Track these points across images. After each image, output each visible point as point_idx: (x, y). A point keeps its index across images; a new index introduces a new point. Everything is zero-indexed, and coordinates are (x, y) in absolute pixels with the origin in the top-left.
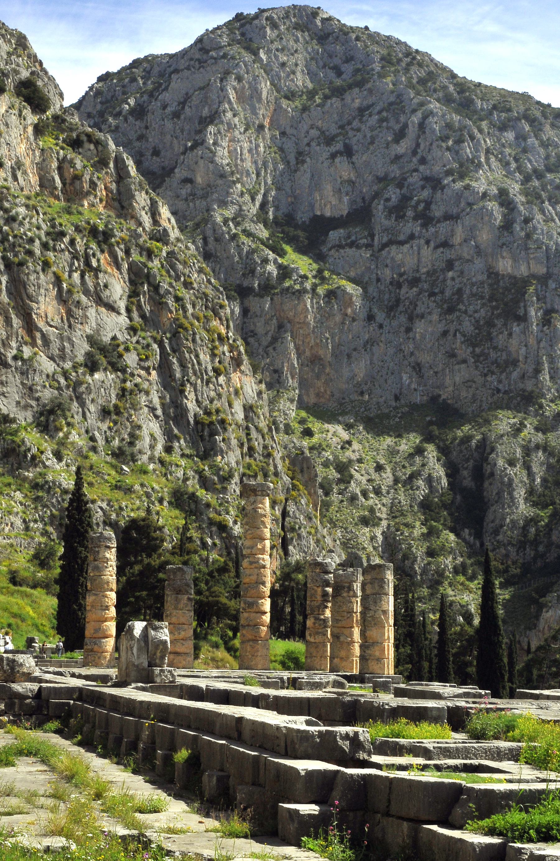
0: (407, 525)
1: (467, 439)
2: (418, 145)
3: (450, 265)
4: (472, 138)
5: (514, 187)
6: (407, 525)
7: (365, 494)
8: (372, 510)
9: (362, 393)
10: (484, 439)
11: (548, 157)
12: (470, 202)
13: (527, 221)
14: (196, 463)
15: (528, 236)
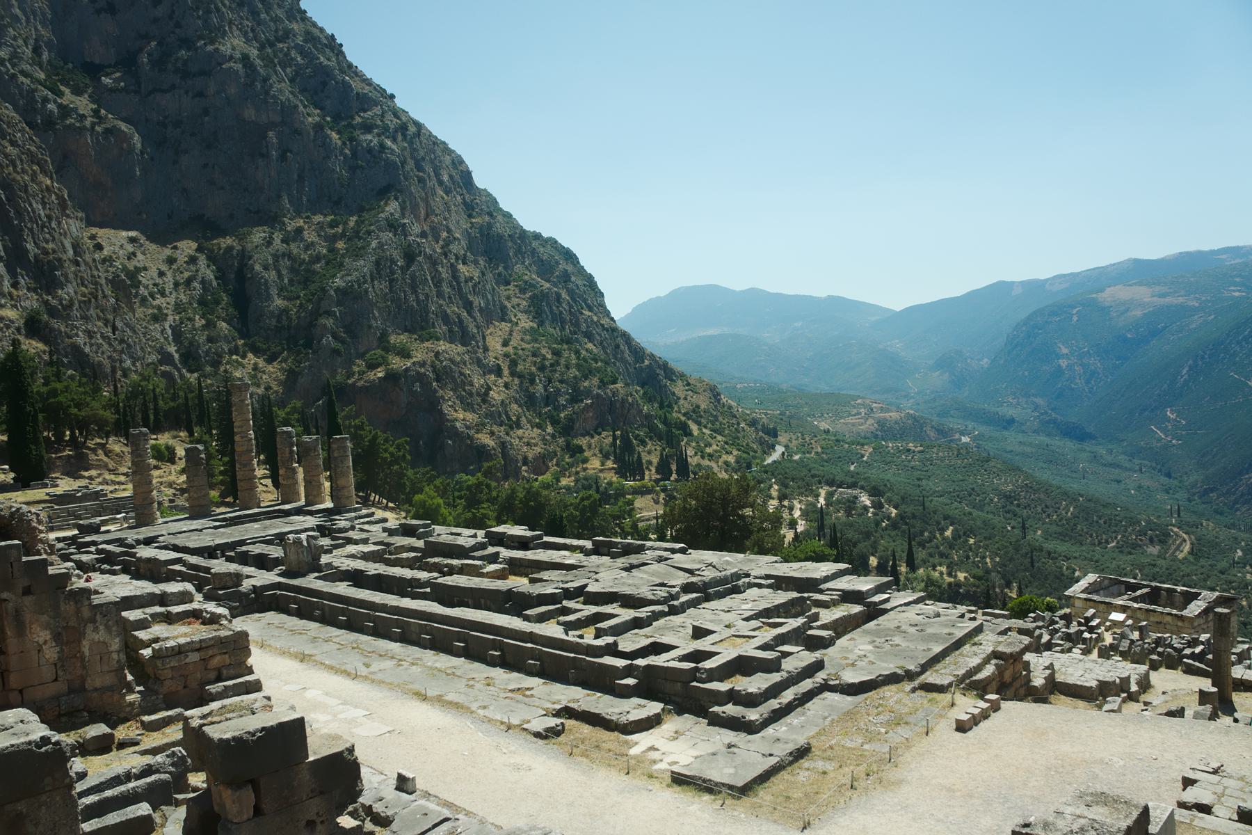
0: (189, 319)
1: (230, 248)
2: (173, 12)
3: (206, 112)
4: (218, 10)
5: (254, 53)
6: (189, 319)
7: (152, 296)
8: (159, 308)
9: (140, 214)
10: (243, 250)
11: (276, 31)
12: (217, 59)
13: (265, 80)
14: (41, 295)
15: (267, 93)
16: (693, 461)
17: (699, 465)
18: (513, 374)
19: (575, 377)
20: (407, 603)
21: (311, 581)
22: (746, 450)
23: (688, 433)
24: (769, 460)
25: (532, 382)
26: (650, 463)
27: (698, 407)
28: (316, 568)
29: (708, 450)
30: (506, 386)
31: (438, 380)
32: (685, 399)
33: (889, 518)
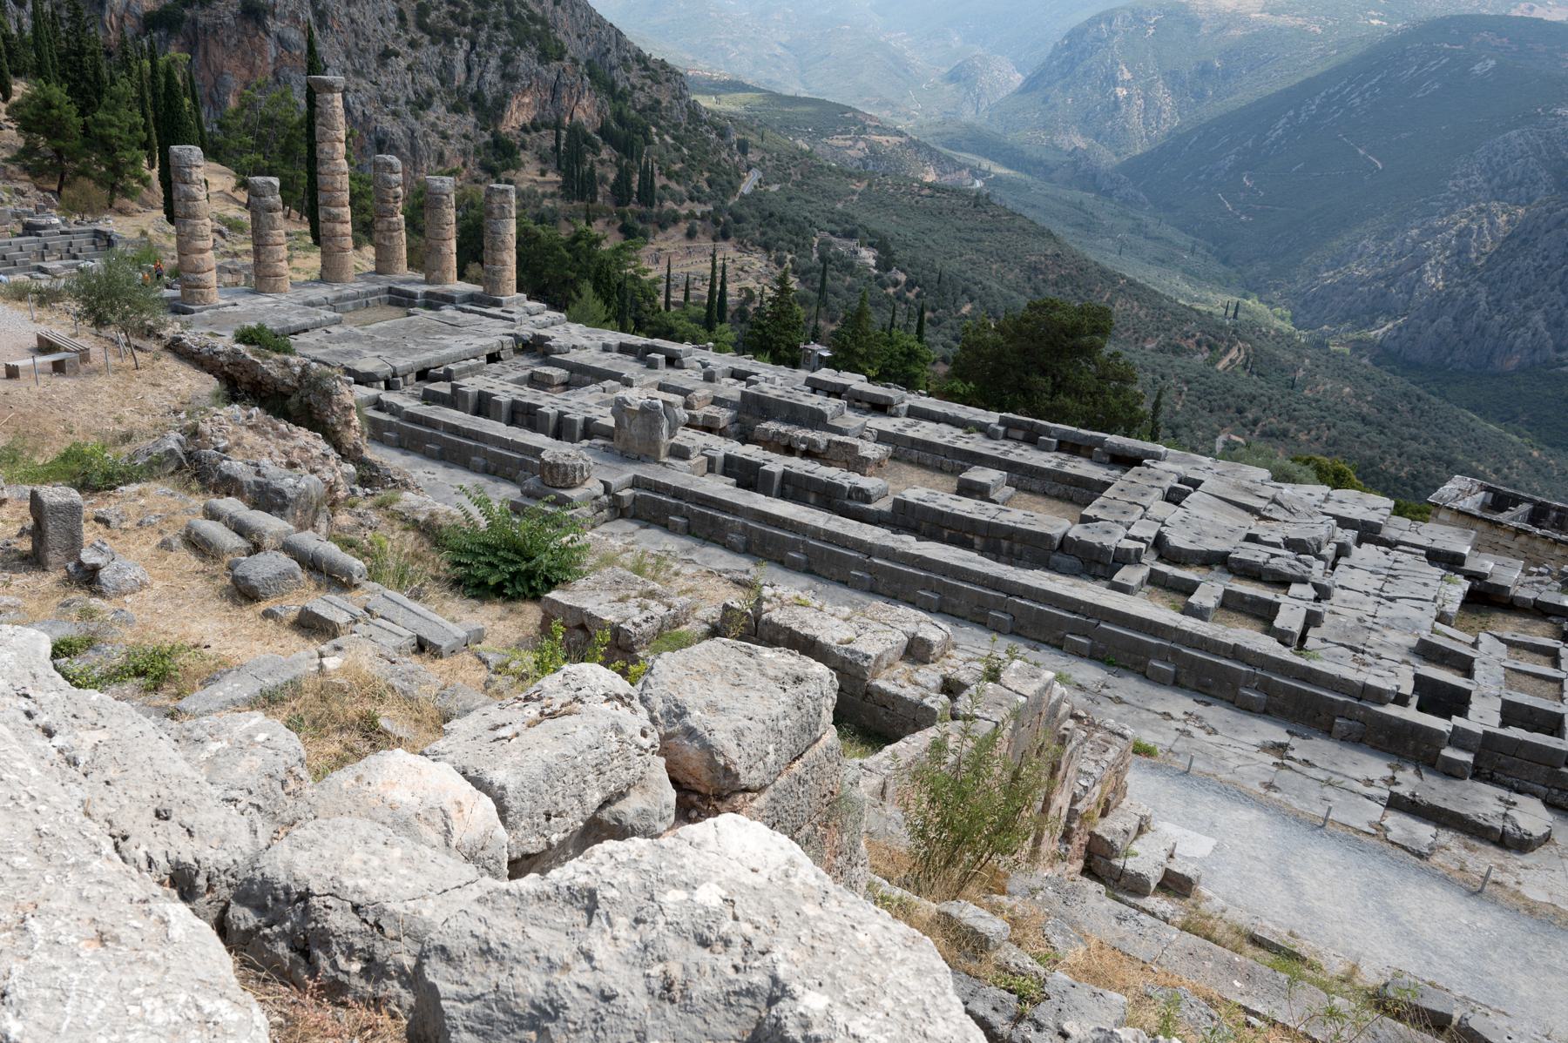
16: (659, 181)
17: (664, 187)
18: (422, 27)
19: (507, 43)
20: (910, 544)
21: (679, 475)
22: (715, 168)
23: (649, 142)
24: (746, 188)
25: (449, 41)
26: (604, 179)
27: (658, 102)
28: (681, 453)
29: (678, 167)
30: (413, 44)
31: (320, 27)
32: (642, 89)
33: (896, 283)
